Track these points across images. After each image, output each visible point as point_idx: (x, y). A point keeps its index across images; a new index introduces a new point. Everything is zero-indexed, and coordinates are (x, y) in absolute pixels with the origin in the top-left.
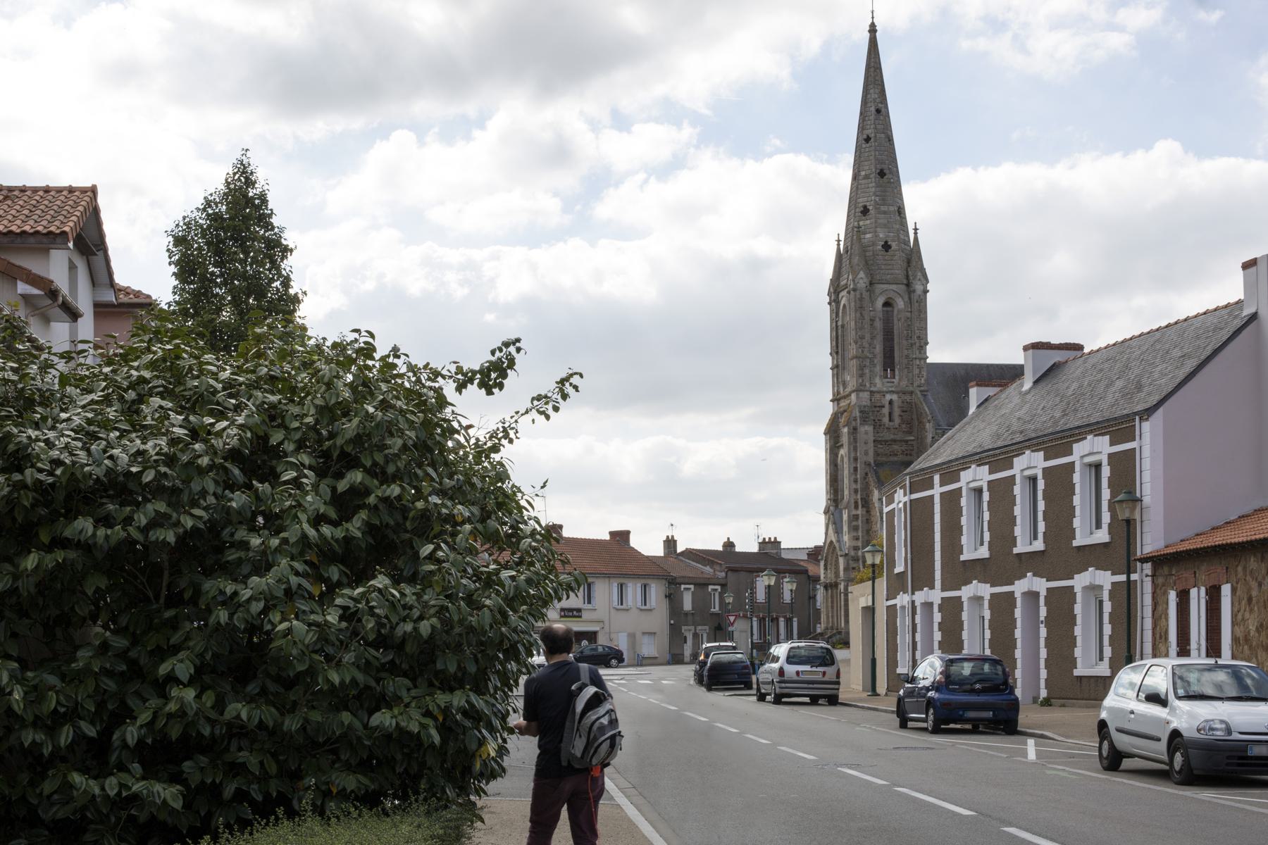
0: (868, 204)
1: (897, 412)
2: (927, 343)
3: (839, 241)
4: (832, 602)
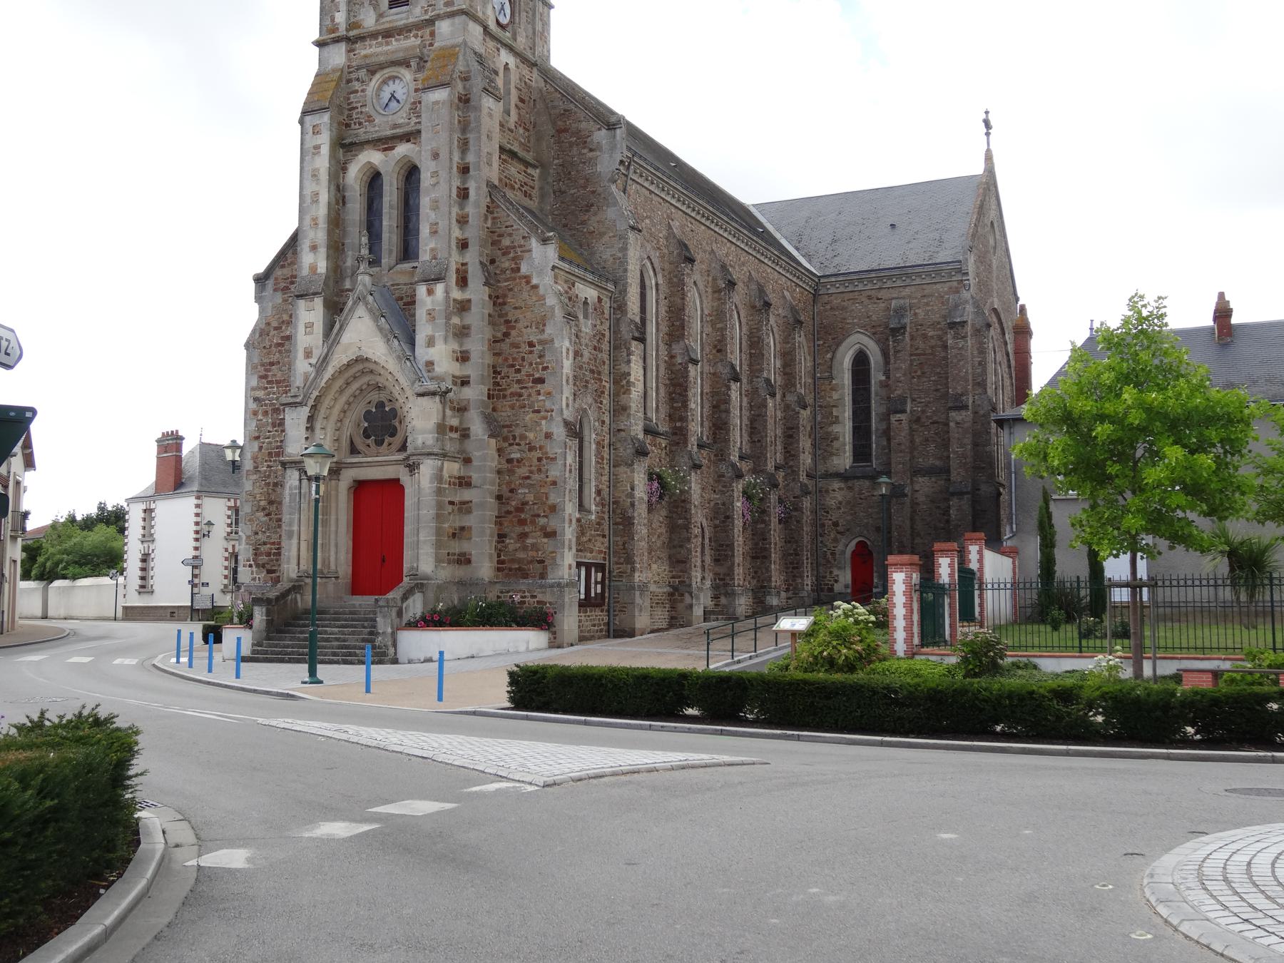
1: (514, 98)
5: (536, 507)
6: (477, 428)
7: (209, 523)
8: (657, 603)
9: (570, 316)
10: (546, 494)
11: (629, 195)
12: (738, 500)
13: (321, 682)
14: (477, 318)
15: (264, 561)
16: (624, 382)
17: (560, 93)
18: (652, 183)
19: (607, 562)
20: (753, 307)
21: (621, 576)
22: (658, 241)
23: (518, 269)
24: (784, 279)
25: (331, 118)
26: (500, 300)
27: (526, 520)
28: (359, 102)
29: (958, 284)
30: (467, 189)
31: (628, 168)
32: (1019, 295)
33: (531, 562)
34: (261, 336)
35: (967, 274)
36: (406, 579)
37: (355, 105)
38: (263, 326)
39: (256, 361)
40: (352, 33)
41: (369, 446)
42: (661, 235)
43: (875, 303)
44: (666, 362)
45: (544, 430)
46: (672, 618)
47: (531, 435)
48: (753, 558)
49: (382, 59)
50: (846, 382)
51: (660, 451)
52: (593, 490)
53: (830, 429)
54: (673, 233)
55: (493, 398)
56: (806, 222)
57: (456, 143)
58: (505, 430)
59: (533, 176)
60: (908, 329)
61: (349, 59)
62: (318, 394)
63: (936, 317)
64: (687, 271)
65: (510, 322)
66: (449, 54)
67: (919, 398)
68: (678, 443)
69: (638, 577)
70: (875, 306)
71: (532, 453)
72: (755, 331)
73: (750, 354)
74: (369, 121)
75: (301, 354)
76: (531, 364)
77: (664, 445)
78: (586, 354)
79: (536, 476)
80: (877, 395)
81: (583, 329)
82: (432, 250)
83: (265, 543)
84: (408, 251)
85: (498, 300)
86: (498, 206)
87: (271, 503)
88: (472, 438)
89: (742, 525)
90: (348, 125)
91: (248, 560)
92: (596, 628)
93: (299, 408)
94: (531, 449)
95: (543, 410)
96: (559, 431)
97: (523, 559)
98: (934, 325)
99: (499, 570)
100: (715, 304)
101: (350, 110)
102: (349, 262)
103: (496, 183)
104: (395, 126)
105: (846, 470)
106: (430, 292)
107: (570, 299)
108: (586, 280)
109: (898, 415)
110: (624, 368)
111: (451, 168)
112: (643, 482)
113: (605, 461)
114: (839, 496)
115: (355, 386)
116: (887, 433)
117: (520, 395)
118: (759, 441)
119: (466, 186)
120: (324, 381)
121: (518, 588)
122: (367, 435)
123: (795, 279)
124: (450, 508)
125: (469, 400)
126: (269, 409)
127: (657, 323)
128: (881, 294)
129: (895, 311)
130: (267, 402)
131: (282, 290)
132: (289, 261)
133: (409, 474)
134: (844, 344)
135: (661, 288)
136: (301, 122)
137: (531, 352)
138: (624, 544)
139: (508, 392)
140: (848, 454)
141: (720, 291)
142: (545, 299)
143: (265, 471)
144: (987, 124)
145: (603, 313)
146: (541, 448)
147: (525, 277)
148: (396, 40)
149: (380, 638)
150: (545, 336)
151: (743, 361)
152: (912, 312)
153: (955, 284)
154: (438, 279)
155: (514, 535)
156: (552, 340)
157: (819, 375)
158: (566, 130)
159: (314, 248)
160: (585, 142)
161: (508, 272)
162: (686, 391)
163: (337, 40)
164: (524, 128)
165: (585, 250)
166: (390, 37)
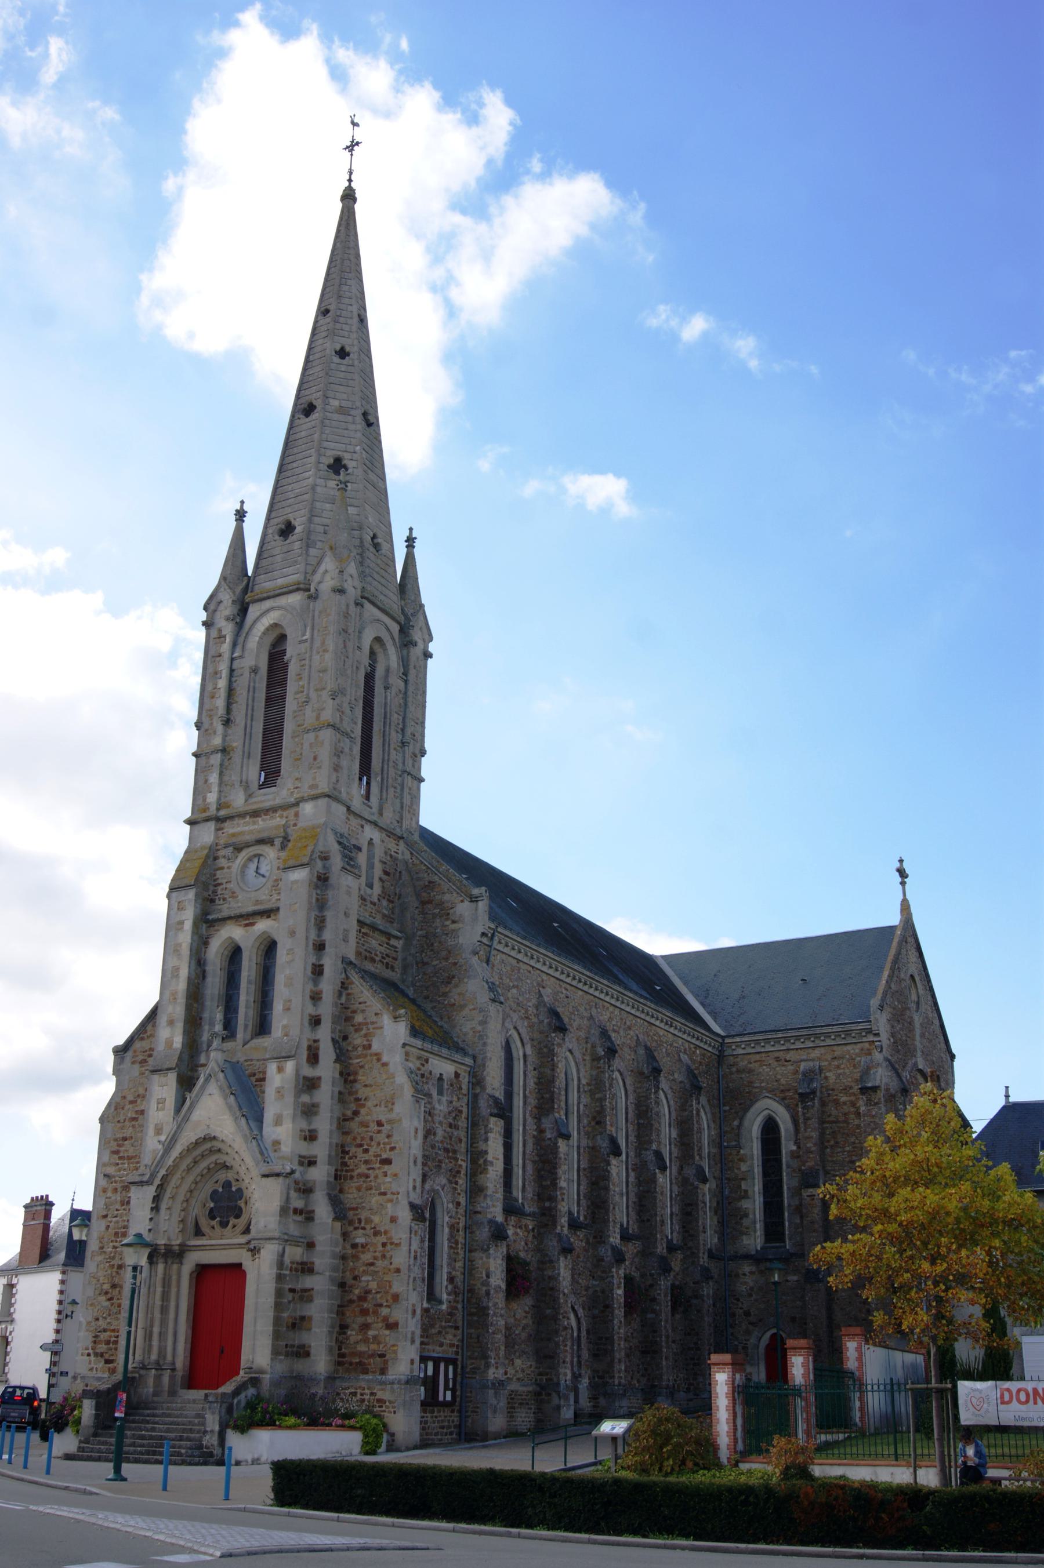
0: (346, 456)
1: (378, 872)
2: (423, 753)
3: (240, 515)
4: (165, 1297)
5: (379, 1296)
6: (323, 1210)
7: (74, 1302)
8: (521, 1404)
9: (420, 1093)
10: (390, 1282)
11: (493, 966)
12: (619, 1288)
13: (125, 1480)
14: (325, 1096)
15: (102, 1350)
16: (481, 1161)
17: (425, 865)
18: (520, 952)
19: (459, 1357)
20: (642, 1073)
21: (474, 1373)
22: (527, 1011)
23: (370, 1046)
24: (680, 1041)
25: (196, 895)
26: (352, 1078)
27: (368, 1310)
28: (225, 878)
29: (870, 1045)
30: (322, 965)
31: (492, 939)
32: (954, 1051)
33: (372, 1356)
34: (116, 1109)
35: (877, 1035)
36: (242, 1372)
37: (219, 881)
38: (118, 1099)
39: (109, 1136)
40: (222, 813)
41: (213, 1227)
42: (530, 1004)
43: (783, 1065)
44: (534, 1136)
45: (390, 1213)
46: (539, 1421)
47: (376, 1219)
48: (643, 1352)
49: (248, 838)
50: (755, 1152)
51: (526, 1234)
52: (445, 1277)
53: (739, 1204)
54: (543, 1001)
55: (340, 1179)
56: (715, 975)
57: (313, 920)
58: (351, 1213)
59: (396, 947)
60: (818, 1094)
61: (217, 837)
62: (165, 1173)
63: (848, 1081)
64: (557, 1040)
65: (361, 1099)
66: (313, 833)
67: (834, 1170)
68: (547, 1225)
69: (493, 1374)
70: (783, 1068)
71: (378, 1238)
72: (642, 1099)
73: (639, 1124)
74: (233, 897)
75: (151, 1131)
76: (379, 1144)
77: (530, 1227)
78: (440, 1133)
79: (379, 1263)
80: (788, 1166)
81: (437, 1106)
82: (285, 1027)
83: (105, 1330)
84: (263, 1027)
85: (347, 1076)
86: (352, 983)
87: (114, 1286)
88: (317, 1221)
89: (623, 1314)
90: (212, 901)
91: (87, 1349)
92: (445, 1430)
93: (145, 1188)
94: (376, 1233)
95: (389, 1192)
96: (405, 1215)
97: (364, 1353)
98: (846, 1089)
99: (339, 1364)
100: (594, 1073)
101: (215, 886)
102: (205, 1037)
103: (353, 958)
104: (257, 902)
105: (757, 1251)
106: (280, 1070)
107: (423, 1076)
108: (440, 1056)
109: (811, 1190)
110: (482, 1146)
111: (307, 946)
112: (500, 1269)
113: (460, 1246)
114: (750, 1281)
115: (203, 1164)
116: (799, 1210)
117: (367, 1176)
118: (648, 1220)
119: (321, 963)
120: (172, 1159)
121: (359, 1384)
122: (212, 1216)
123: (694, 1041)
124: (290, 1296)
125: (315, 1182)
126: (119, 1186)
127: (525, 1096)
128: (790, 1056)
129: (804, 1074)
130: (117, 1178)
131: (141, 1063)
132: (149, 1033)
133: (251, 1259)
134: (753, 1110)
135: (530, 1059)
136: (168, 896)
137: (379, 1132)
138: (478, 1337)
139: (355, 1173)
140: (758, 1233)
141: (599, 1059)
142: (394, 1077)
143: (111, 1253)
144: (902, 873)
145: (461, 1088)
146: (386, 1232)
147: (376, 1054)
148: (263, 820)
149: (208, 1437)
150: (393, 1116)
151: (630, 1133)
152: (823, 1075)
153: (867, 1045)
154: (288, 1057)
155: (356, 1327)
156: (400, 1120)
157: (725, 1144)
158: (430, 902)
159: (171, 1023)
160: (448, 914)
161: (359, 1049)
162: (555, 1168)
163: (207, 820)
164: (388, 900)
165: (446, 1022)
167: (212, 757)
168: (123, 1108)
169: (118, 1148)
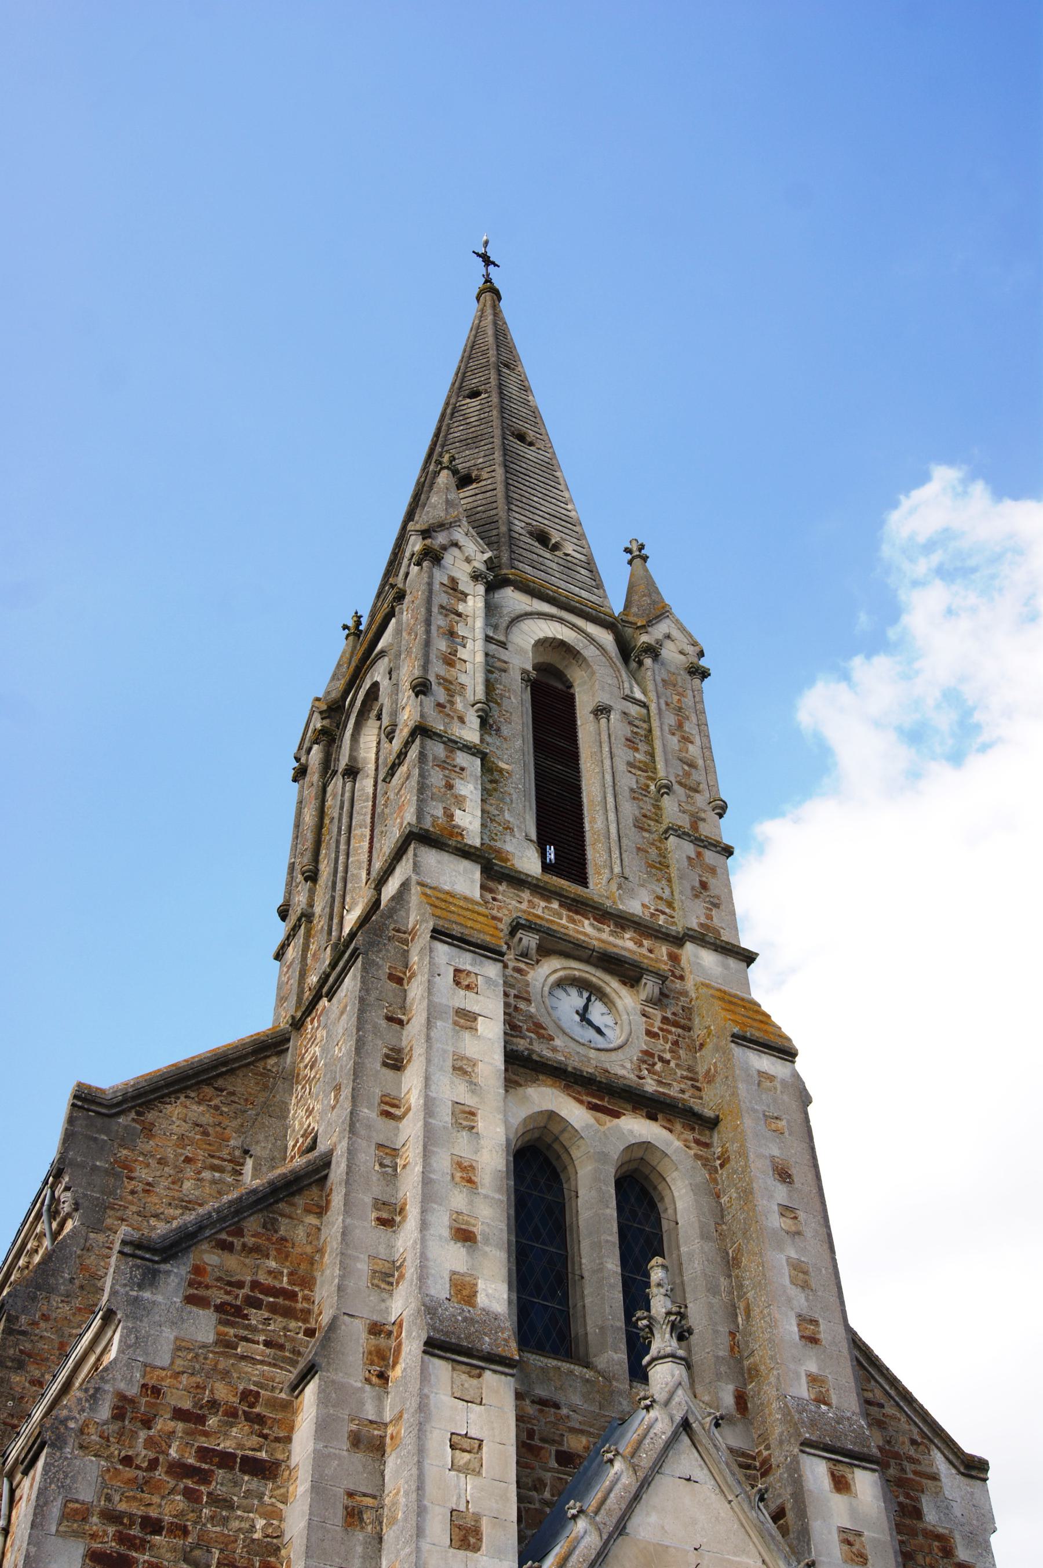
34: (119, 1414)
39: (86, 1493)
74: (541, 1036)
82: (813, 1380)
106: (841, 1484)
131: (220, 1308)
148: (592, 925)
159: (464, 1236)
166: (577, 913)
167: (459, 753)
168: (147, 1424)
169: (122, 1550)
